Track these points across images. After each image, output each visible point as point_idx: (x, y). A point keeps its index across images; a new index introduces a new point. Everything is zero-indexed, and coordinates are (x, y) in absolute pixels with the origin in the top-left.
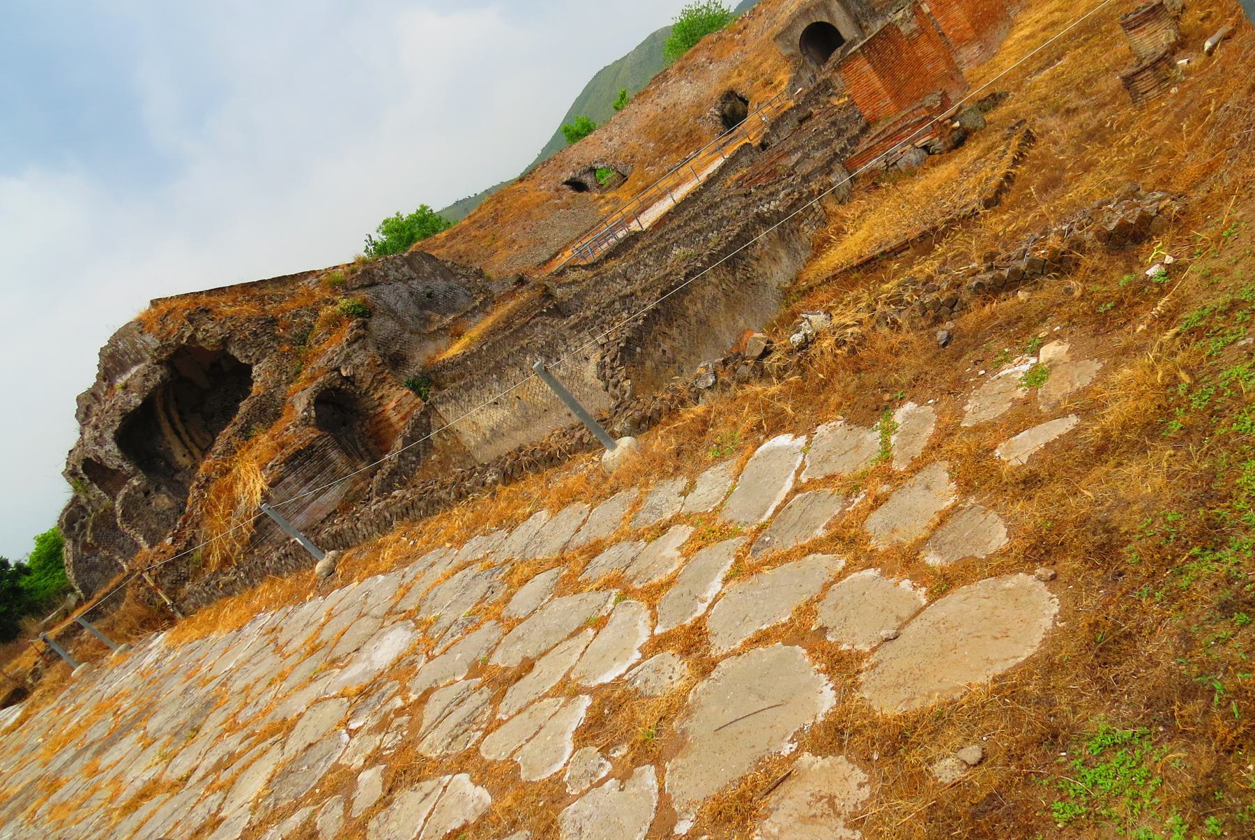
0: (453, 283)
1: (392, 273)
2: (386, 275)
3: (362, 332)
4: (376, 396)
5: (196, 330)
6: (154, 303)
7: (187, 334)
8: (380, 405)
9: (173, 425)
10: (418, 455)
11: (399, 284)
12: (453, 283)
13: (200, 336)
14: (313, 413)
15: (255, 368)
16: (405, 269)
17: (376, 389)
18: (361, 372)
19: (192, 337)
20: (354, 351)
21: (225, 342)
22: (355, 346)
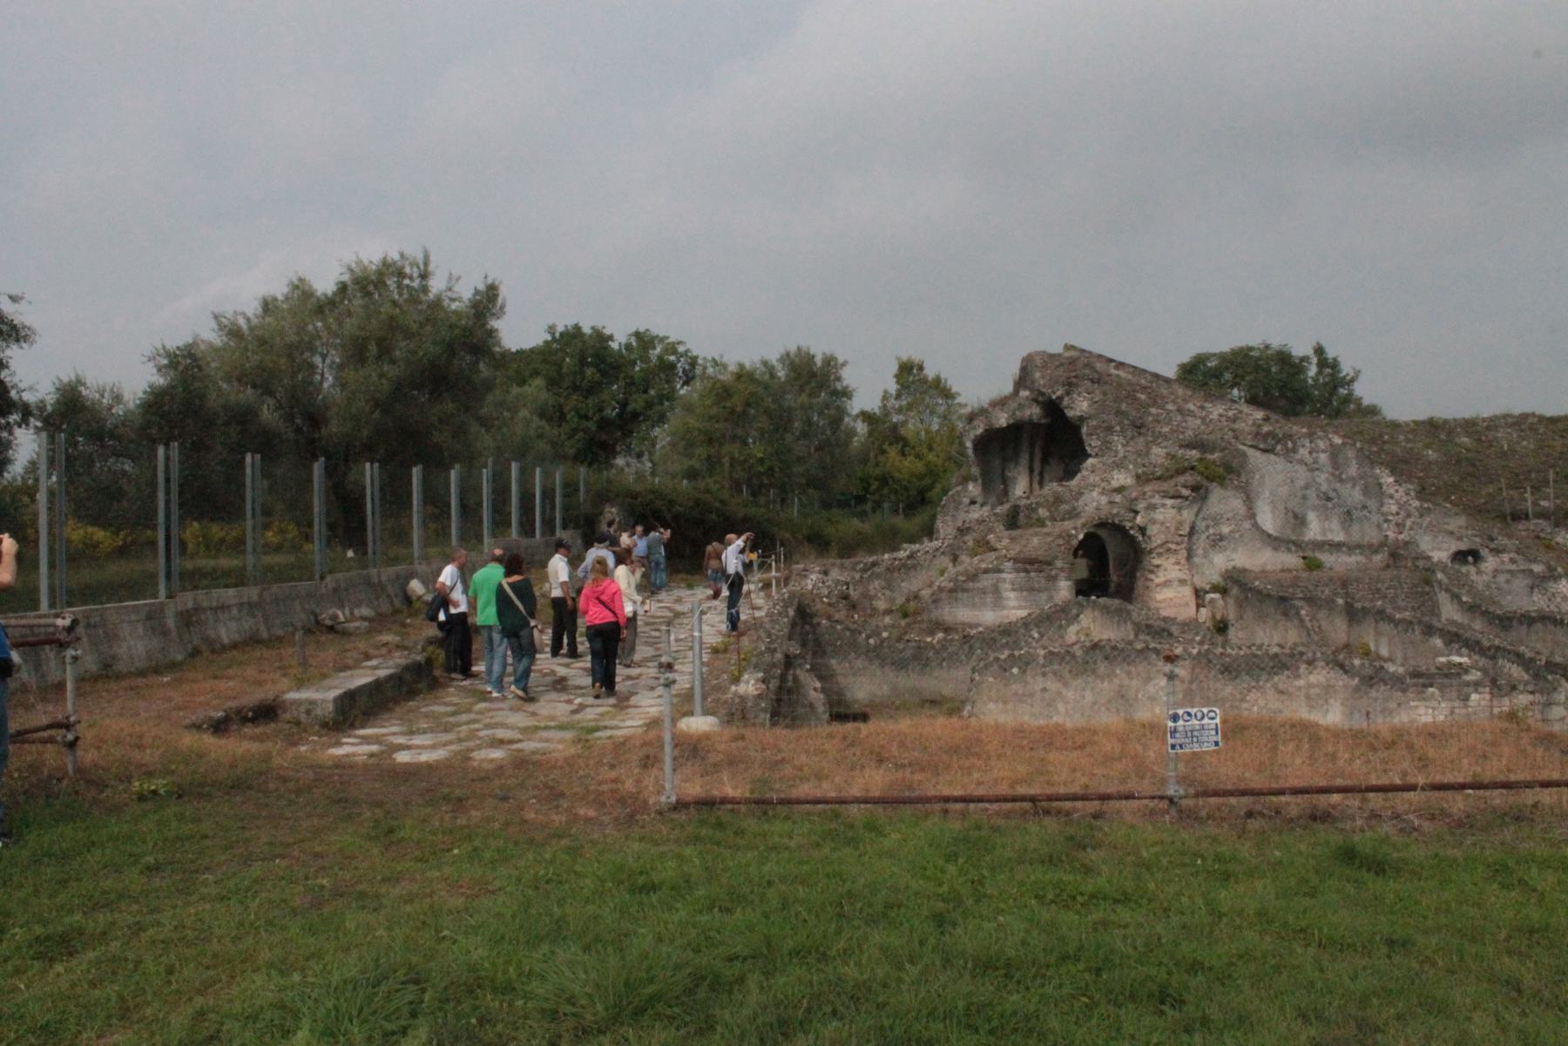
0: (1372, 504)
1: (1303, 453)
2: (1294, 450)
3: (1185, 492)
4: (1156, 562)
5: (1068, 393)
6: (1068, 347)
7: (1059, 393)
8: (1152, 572)
9: (1031, 461)
10: (1042, 636)
11: (1301, 469)
12: (1372, 504)
13: (1066, 402)
14: (1081, 537)
15: (1090, 461)
16: (1323, 457)
17: (1160, 555)
18: (1153, 530)
19: (1060, 398)
20: (1164, 505)
21: (1082, 419)
22: (1169, 502)
